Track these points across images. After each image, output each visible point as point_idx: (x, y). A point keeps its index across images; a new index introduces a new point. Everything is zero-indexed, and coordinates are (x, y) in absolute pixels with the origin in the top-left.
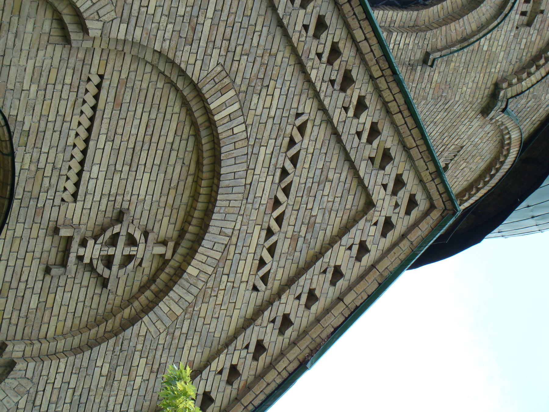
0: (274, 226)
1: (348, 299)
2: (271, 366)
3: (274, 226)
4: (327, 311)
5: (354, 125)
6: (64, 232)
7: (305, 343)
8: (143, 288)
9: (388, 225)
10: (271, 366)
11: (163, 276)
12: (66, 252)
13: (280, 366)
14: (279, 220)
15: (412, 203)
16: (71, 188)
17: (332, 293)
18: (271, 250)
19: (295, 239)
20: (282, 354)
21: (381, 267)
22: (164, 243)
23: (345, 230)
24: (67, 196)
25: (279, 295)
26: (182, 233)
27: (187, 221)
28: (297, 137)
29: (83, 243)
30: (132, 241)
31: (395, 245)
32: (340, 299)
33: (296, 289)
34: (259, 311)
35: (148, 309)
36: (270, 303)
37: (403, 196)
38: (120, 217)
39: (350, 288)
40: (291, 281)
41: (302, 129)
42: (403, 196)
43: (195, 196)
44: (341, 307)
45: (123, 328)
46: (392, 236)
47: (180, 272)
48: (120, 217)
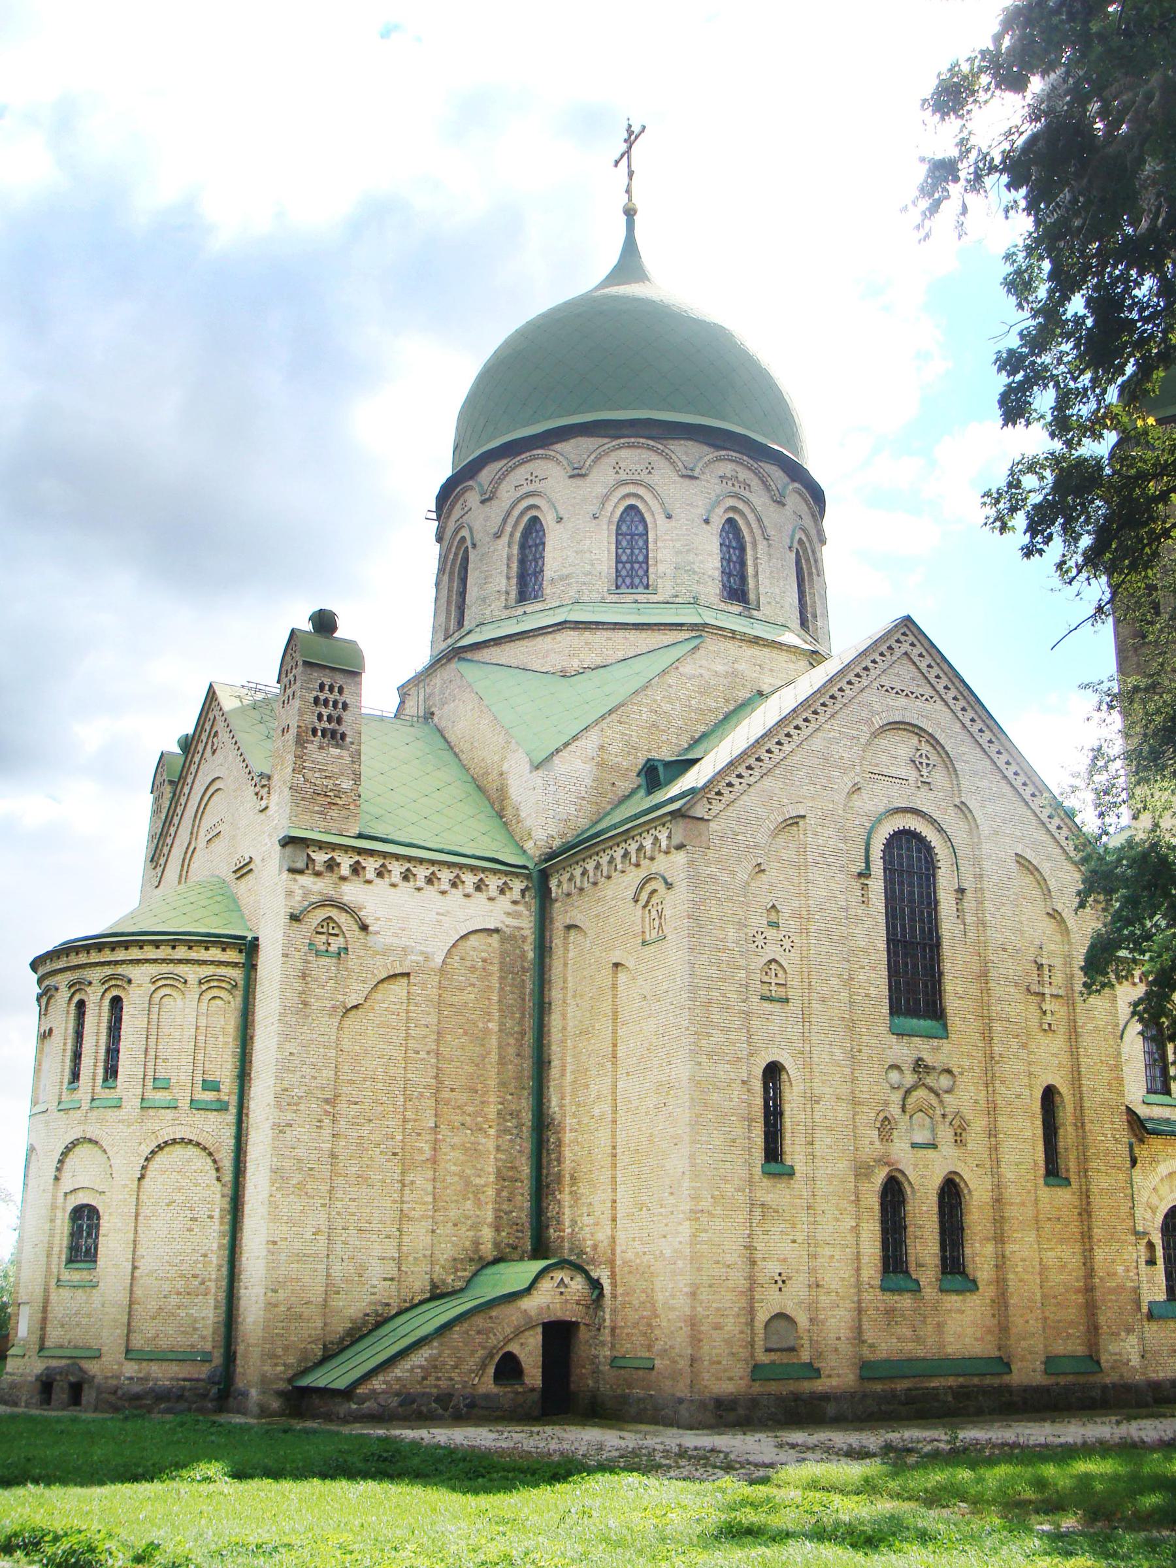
0: (914, 695)
1: (938, 661)
2: (961, 693)
3: (914, 695)
4: (943, 670)
5: (881, 663)
6: (919, 784)
7: (954, 680)
8: (936, 749)
9: (912, 645)
10: (961, 693)
11: (932, 741)
12: (924, 782)
13: (961, 689)
14: (912, 693)
15: (904, 634)
16: (904, 782)
17: (936, 667)
18: (922, 695)
19: (918, 686)
20: (957, 688)
21: (927, 647)
22: (920, 741)
23: (914, 663)
24: (907, 783)
25: (937, 691)
26: (917, 734)
27: (913, 732)
28: (885, 688)
29: (922, 776)
30: (921, 756)
31: (919, 641)
32: (938, 664)
33: (935, 684)
34: (943, 700)
35: (943, 748)
36: (940, 695)
37: (903, 638)
38: (914, 761)
39: (934, 660)
40: (933, 686)
41: (882, 686)
42: (903, 638)
43: (905, 730)
44: (941, 664)
45: (949, 757)
46: (916, 642)
47: (931, 735)
48: (914, 761)
